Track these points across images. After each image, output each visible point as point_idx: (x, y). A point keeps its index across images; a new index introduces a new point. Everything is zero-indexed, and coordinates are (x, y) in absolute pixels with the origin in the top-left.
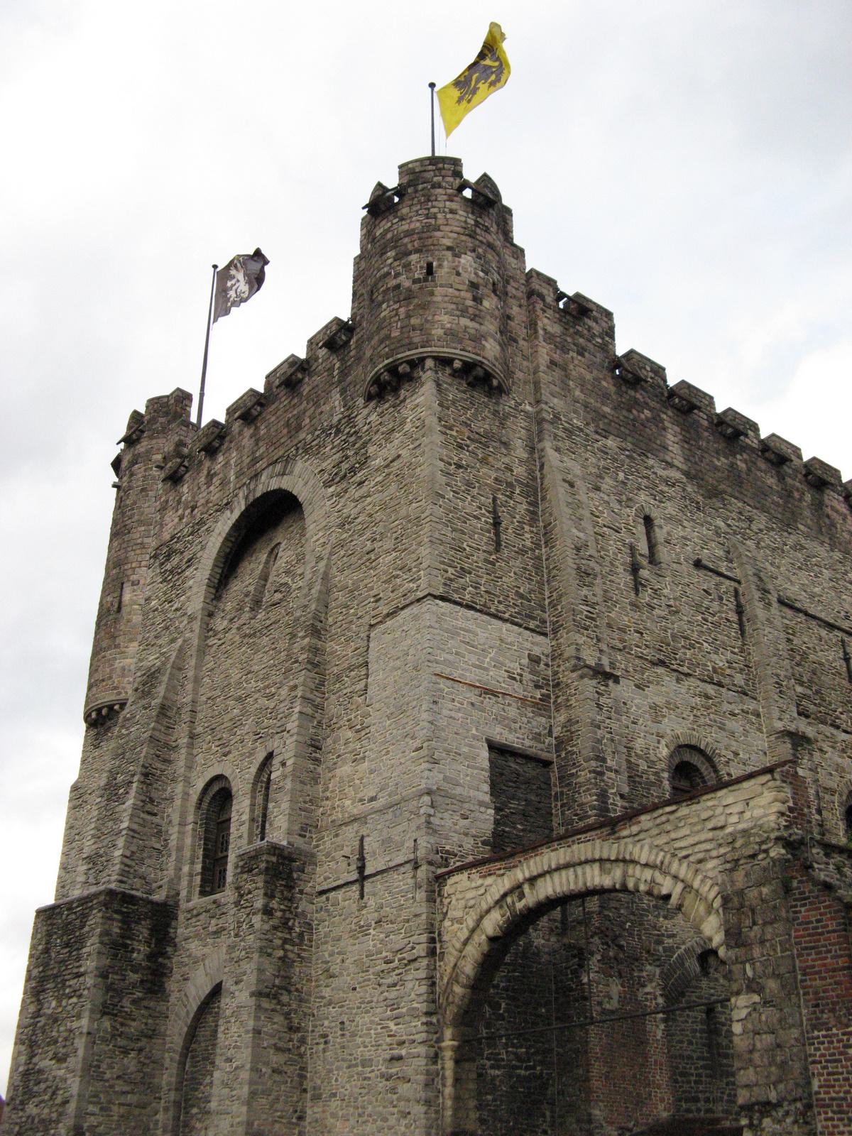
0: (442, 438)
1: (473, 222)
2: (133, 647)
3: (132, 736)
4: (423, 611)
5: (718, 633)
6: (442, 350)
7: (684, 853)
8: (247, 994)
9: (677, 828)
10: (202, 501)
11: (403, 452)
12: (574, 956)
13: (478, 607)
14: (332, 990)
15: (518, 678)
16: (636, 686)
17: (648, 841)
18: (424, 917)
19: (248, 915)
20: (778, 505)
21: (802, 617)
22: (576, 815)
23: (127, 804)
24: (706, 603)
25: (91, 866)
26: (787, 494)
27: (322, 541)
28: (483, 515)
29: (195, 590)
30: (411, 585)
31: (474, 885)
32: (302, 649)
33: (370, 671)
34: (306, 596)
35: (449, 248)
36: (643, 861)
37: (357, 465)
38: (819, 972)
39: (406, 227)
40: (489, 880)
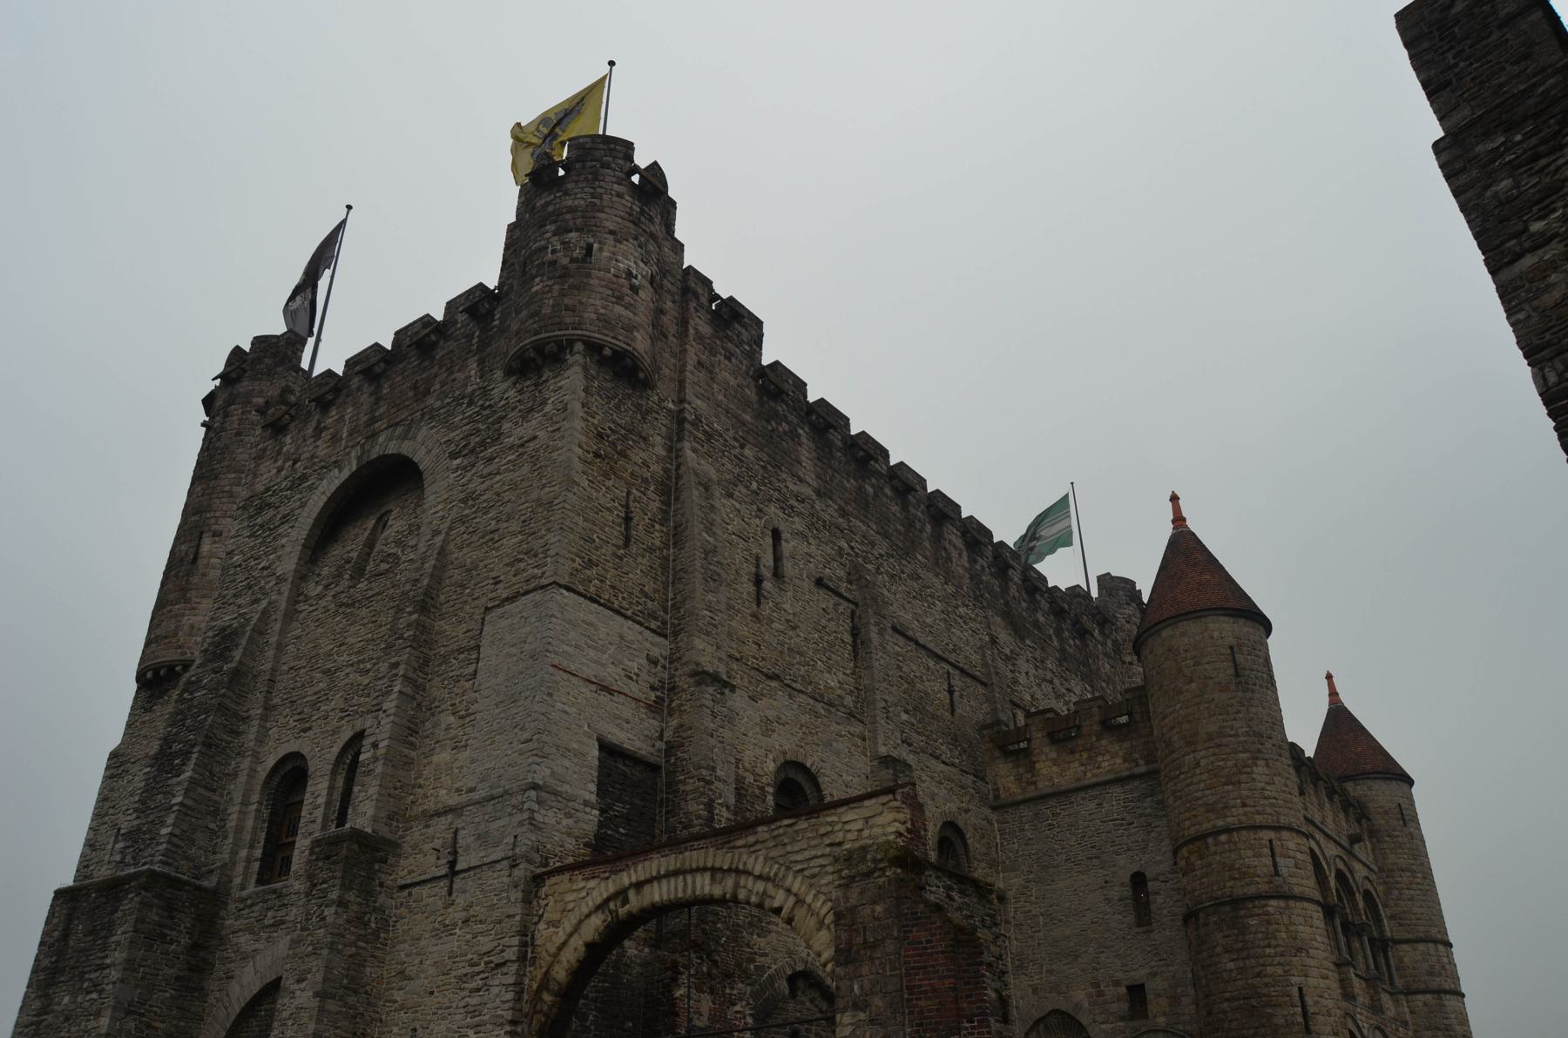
0: (583, 424)
1: (638, 210)
2: (206, 605)
3: (195, 703)
4: (546, 598)
5: (832, 652)
6: (593, 335)
7: (799, 867)
8: (310, 993)
9: (794, 841)
10: (307, 455)
11: (541, 434)
12: (667, 969)
13: (602, 601)
14: (406, 993)
15: (635, 677)
16: (749, 697)
17: (763, 852)
18: (518, 918)
19: (321, 906)
20: (900, 533)
21: (912, 646)
22: (681, 823)
23: (182, 777)
24: (823, 622)
25: (129, 844)
26: (909, 523)
27: (441, 514)
28: (616, 508)
29: (288, 549)
30: (536, 571)
31: (575, 887)
32: (409, 625)
33: (482, 656)
34: (418, 569)
35: (612, 232)
36: (757, 873)
37: (489, 440)
38: (924, 992)
39: (570, 203)
40: (592, 883)
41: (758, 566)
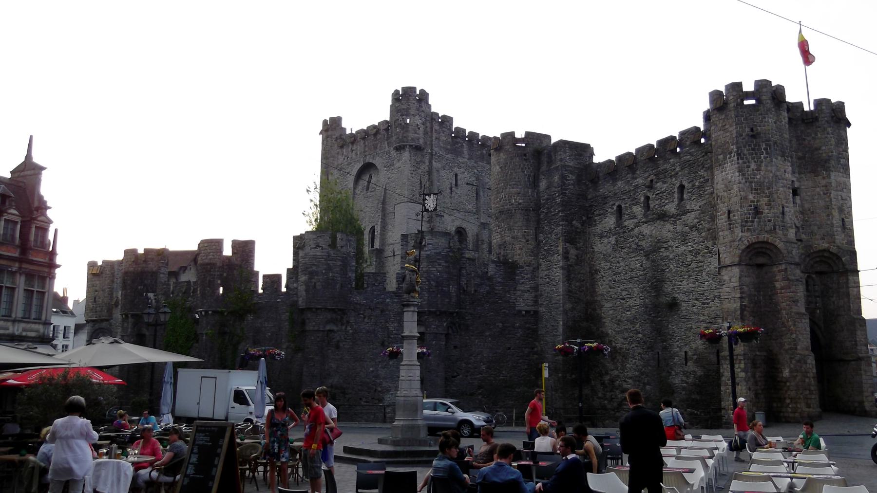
41: (451, 185)
